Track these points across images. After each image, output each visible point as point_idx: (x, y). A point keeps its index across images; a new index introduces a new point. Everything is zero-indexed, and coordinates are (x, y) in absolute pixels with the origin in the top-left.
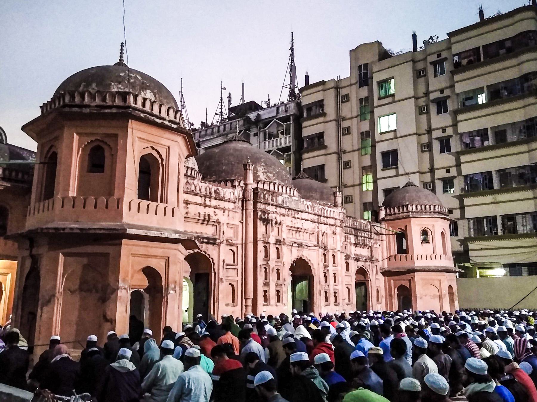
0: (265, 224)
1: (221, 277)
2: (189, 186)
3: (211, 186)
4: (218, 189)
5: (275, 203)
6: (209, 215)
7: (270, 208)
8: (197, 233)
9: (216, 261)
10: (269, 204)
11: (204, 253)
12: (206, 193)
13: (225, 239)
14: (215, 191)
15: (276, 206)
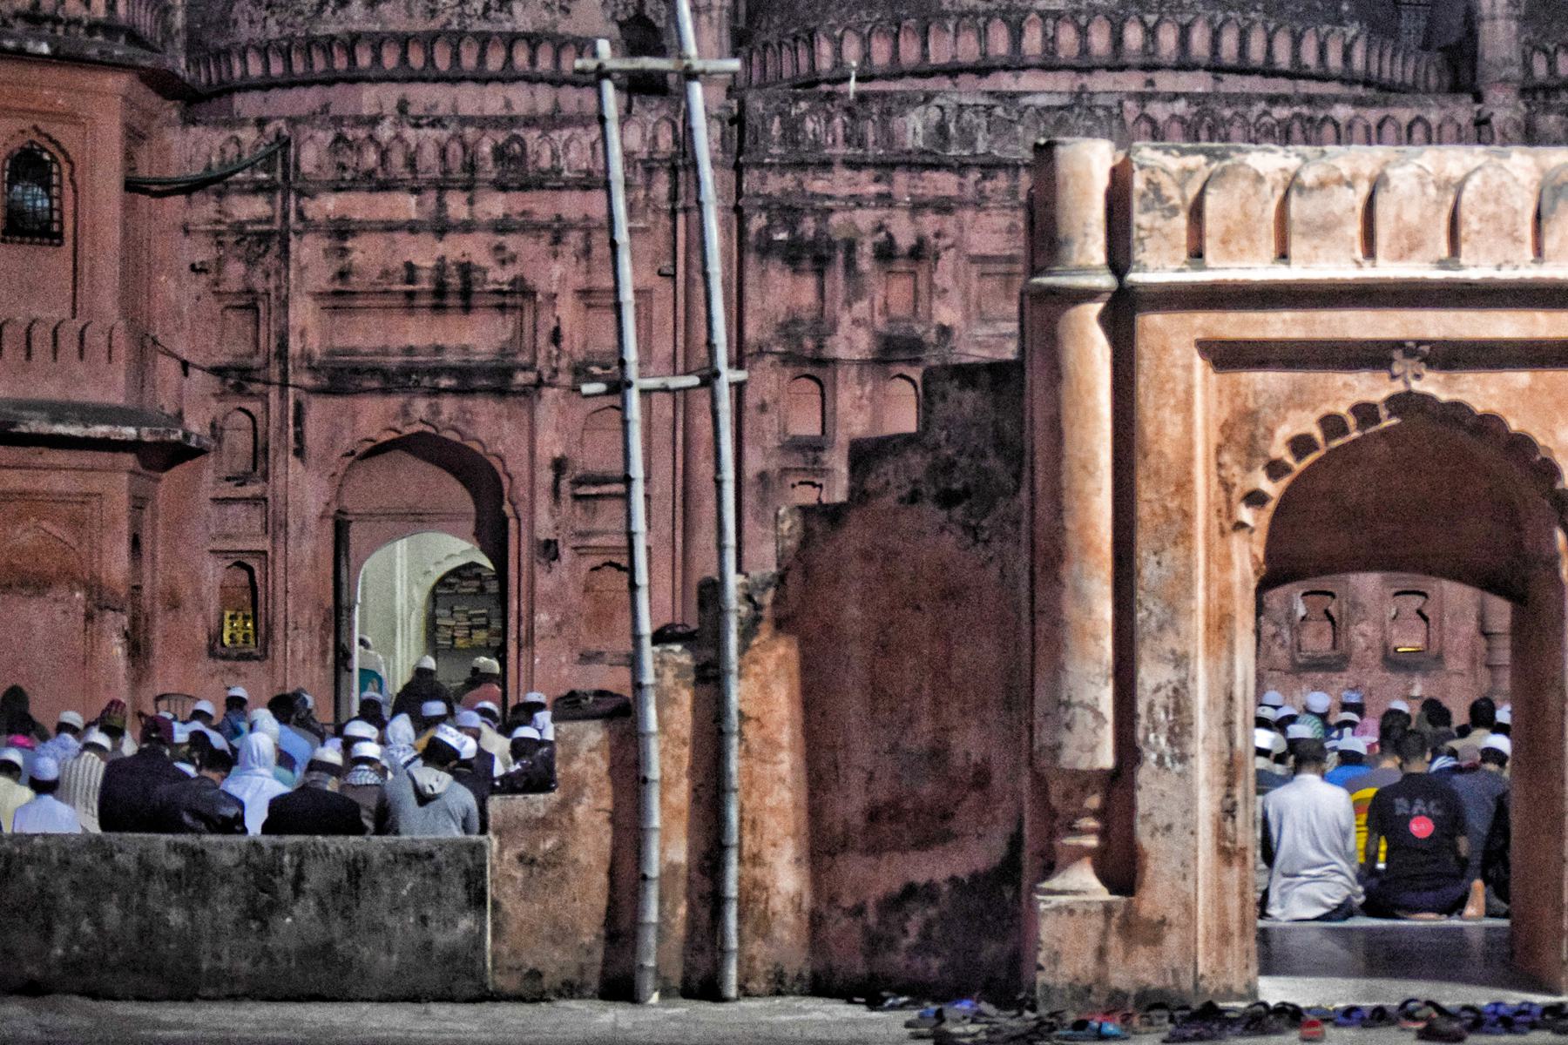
0: (806, 264)
1: (544, 525)
2: (349, 158)
3: (470, 132)
4: (517, 139)
5: (875, 151)
6: (466, 269)
7: (839, 183)
8: (410, 350)
9: (517, 466)
10: (826, 165)
11: (455, 437)
12: (446, 172)
13: (564, 362)
14: (499, 153)
15: (885, 167)
